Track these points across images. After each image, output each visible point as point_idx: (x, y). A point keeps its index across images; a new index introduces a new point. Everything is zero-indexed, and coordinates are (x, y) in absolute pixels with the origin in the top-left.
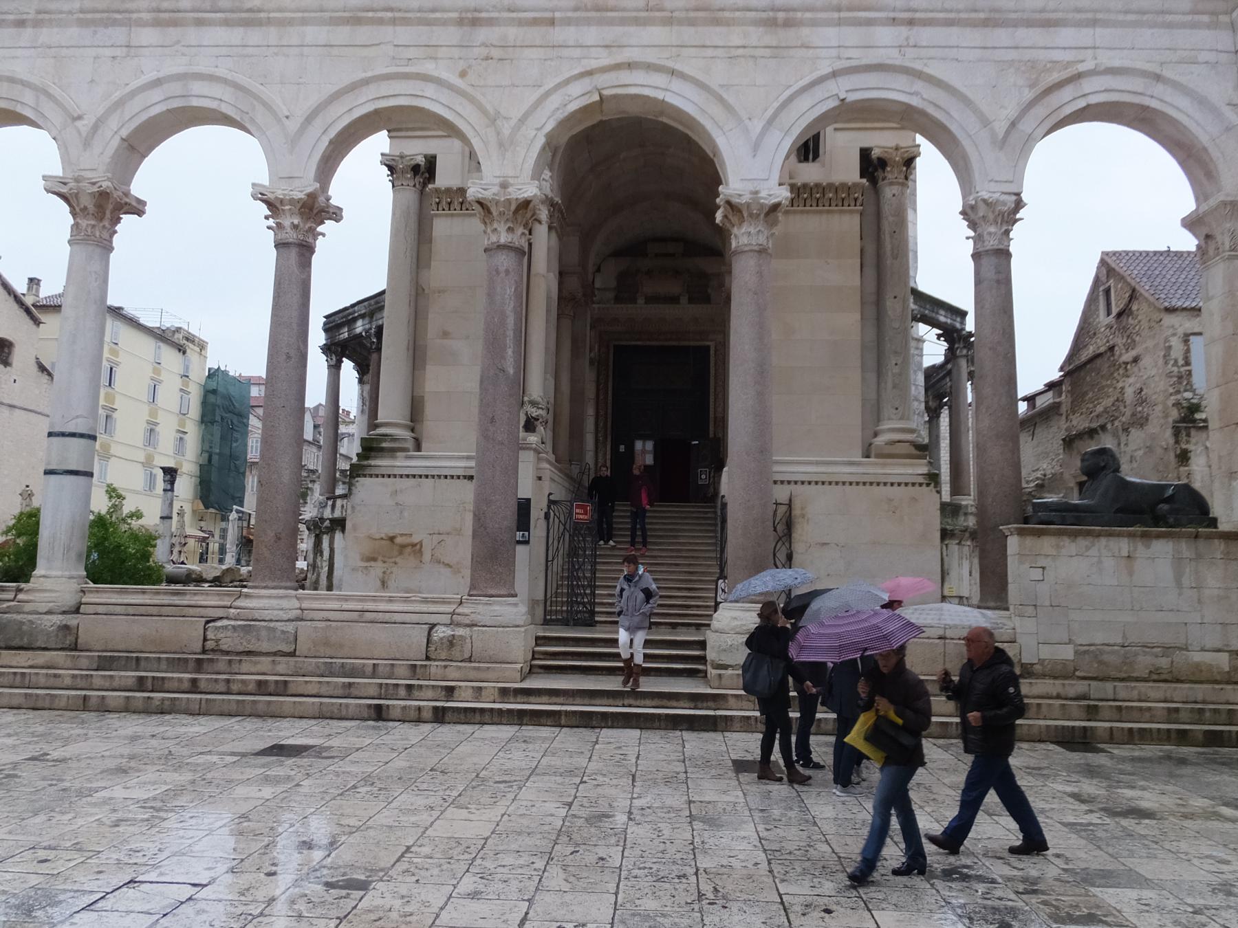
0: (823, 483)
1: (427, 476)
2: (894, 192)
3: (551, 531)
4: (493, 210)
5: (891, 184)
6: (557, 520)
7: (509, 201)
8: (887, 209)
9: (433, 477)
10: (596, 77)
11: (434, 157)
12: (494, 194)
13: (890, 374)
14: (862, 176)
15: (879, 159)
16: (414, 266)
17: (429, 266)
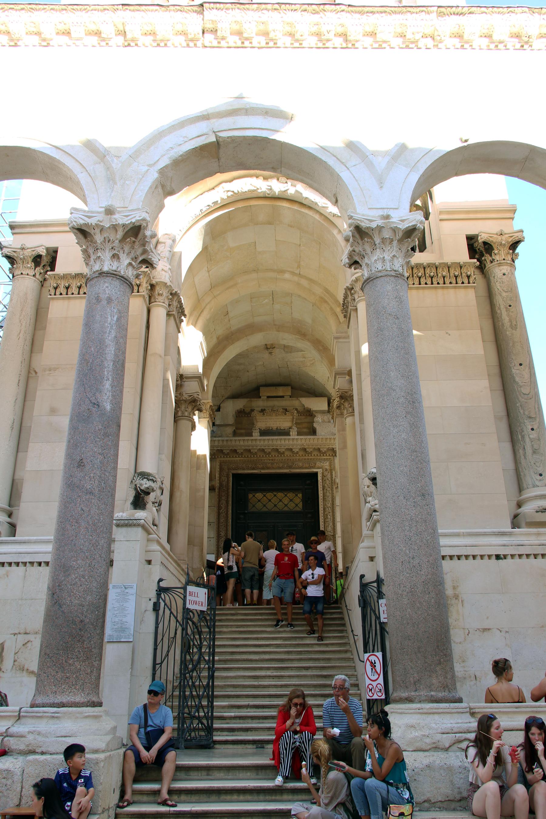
0: (474, 557)
1: (17, 564)
2: (503, 271)
3: (161, 626)
4: (98, 238)
5: (500, 264)
6: (167, 612)
7: (114, 227)
8: (497, 287)
9: (25, 564)
10: (213, 121)
11: (56, 251)
12: (99, 221)
13: (527, 440)
14: (470, 258)
15: (485, 243)
16: (28, 348)
17: (41, 351)
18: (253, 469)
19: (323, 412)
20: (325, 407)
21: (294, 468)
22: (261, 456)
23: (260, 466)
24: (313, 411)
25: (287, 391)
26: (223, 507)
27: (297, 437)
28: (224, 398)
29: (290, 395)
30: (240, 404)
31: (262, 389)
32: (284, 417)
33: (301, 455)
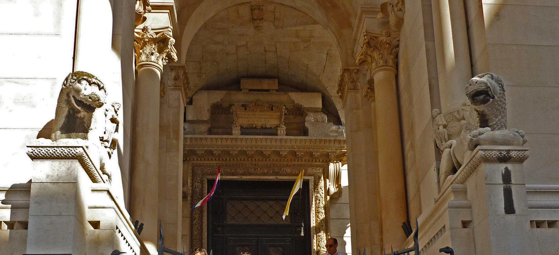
18: (233, 175)
19: (315, 110)
20: (319, 104)
21: (281, 175)
22: (243, 159)
23: (240, 171)
24: (304, 108)
25: (274, 85)
26: (197, 217)
27: (285, 137)
28: (197, 89)
29: (277, 89)
30: (218, 96)
31: (243, 81)
32: (270, 113)
33: (289, 160)
